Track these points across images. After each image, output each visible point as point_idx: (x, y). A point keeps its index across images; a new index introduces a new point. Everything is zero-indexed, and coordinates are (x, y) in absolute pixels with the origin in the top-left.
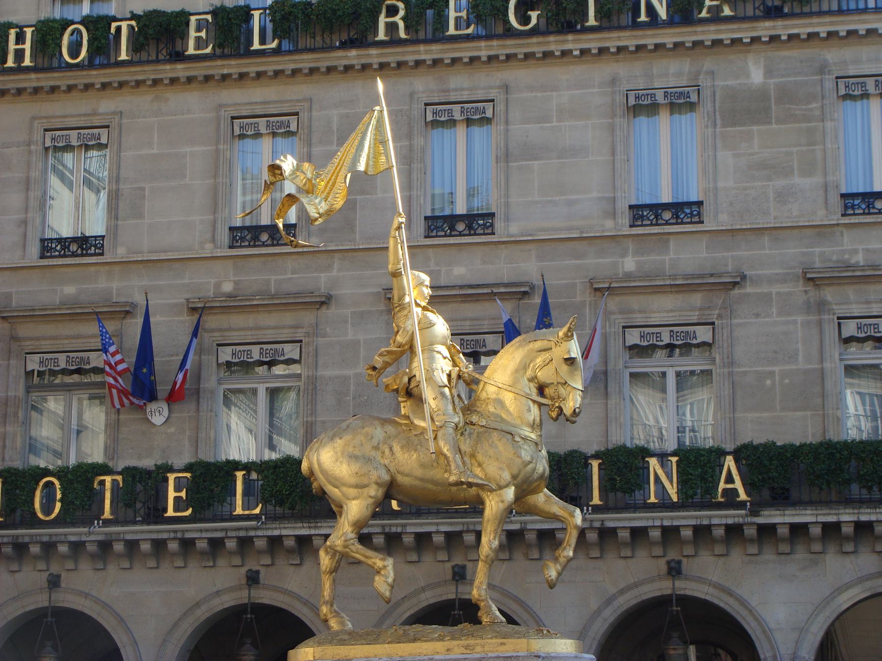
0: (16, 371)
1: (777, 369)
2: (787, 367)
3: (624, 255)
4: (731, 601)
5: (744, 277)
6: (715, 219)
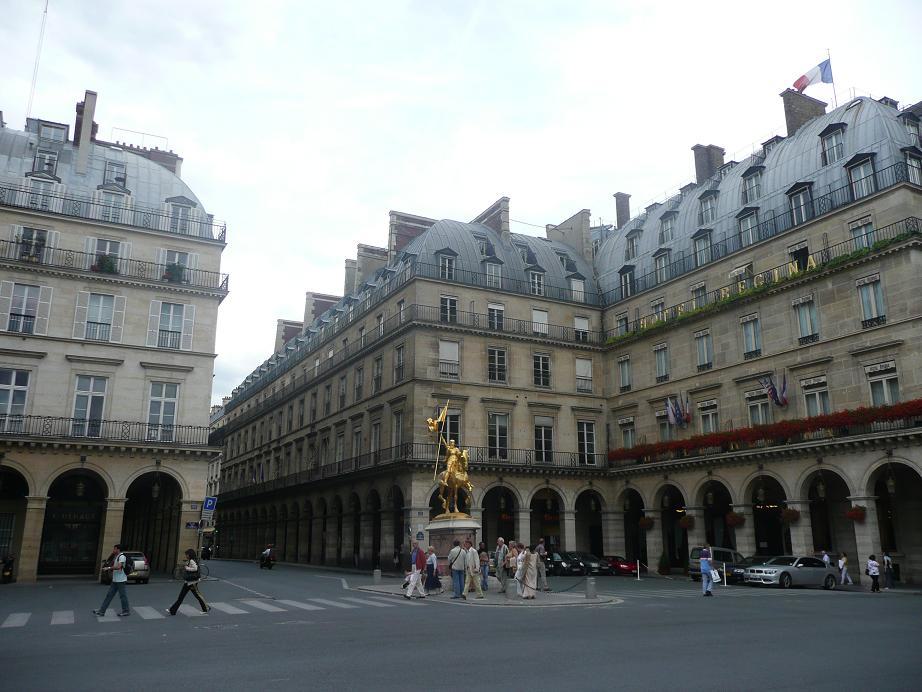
6: (823, 338)
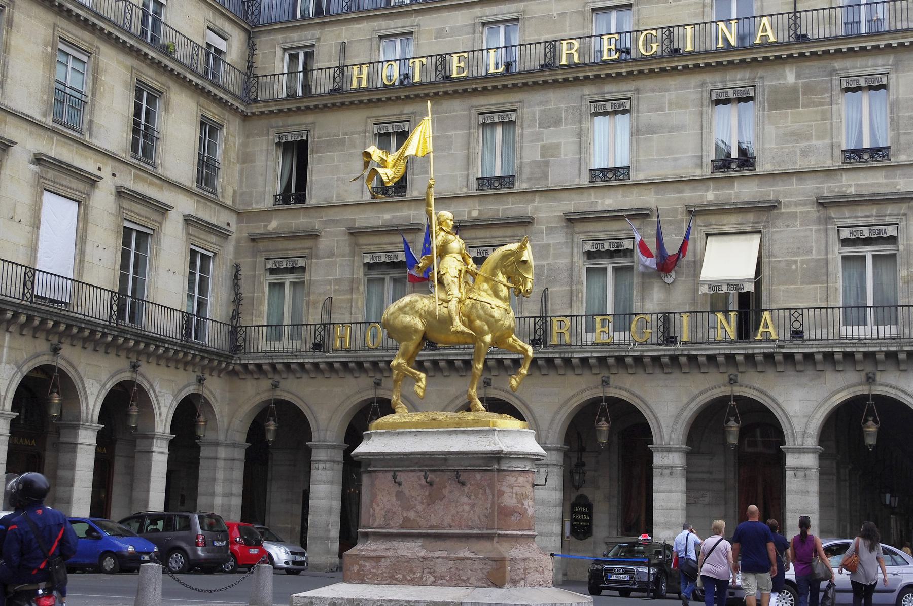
0: (358, 263)
1: (799, 259)
2: (805, 258)
3: (707, 191)
4: (767, 399)
5: (779, 203)
6: (763, 166)
